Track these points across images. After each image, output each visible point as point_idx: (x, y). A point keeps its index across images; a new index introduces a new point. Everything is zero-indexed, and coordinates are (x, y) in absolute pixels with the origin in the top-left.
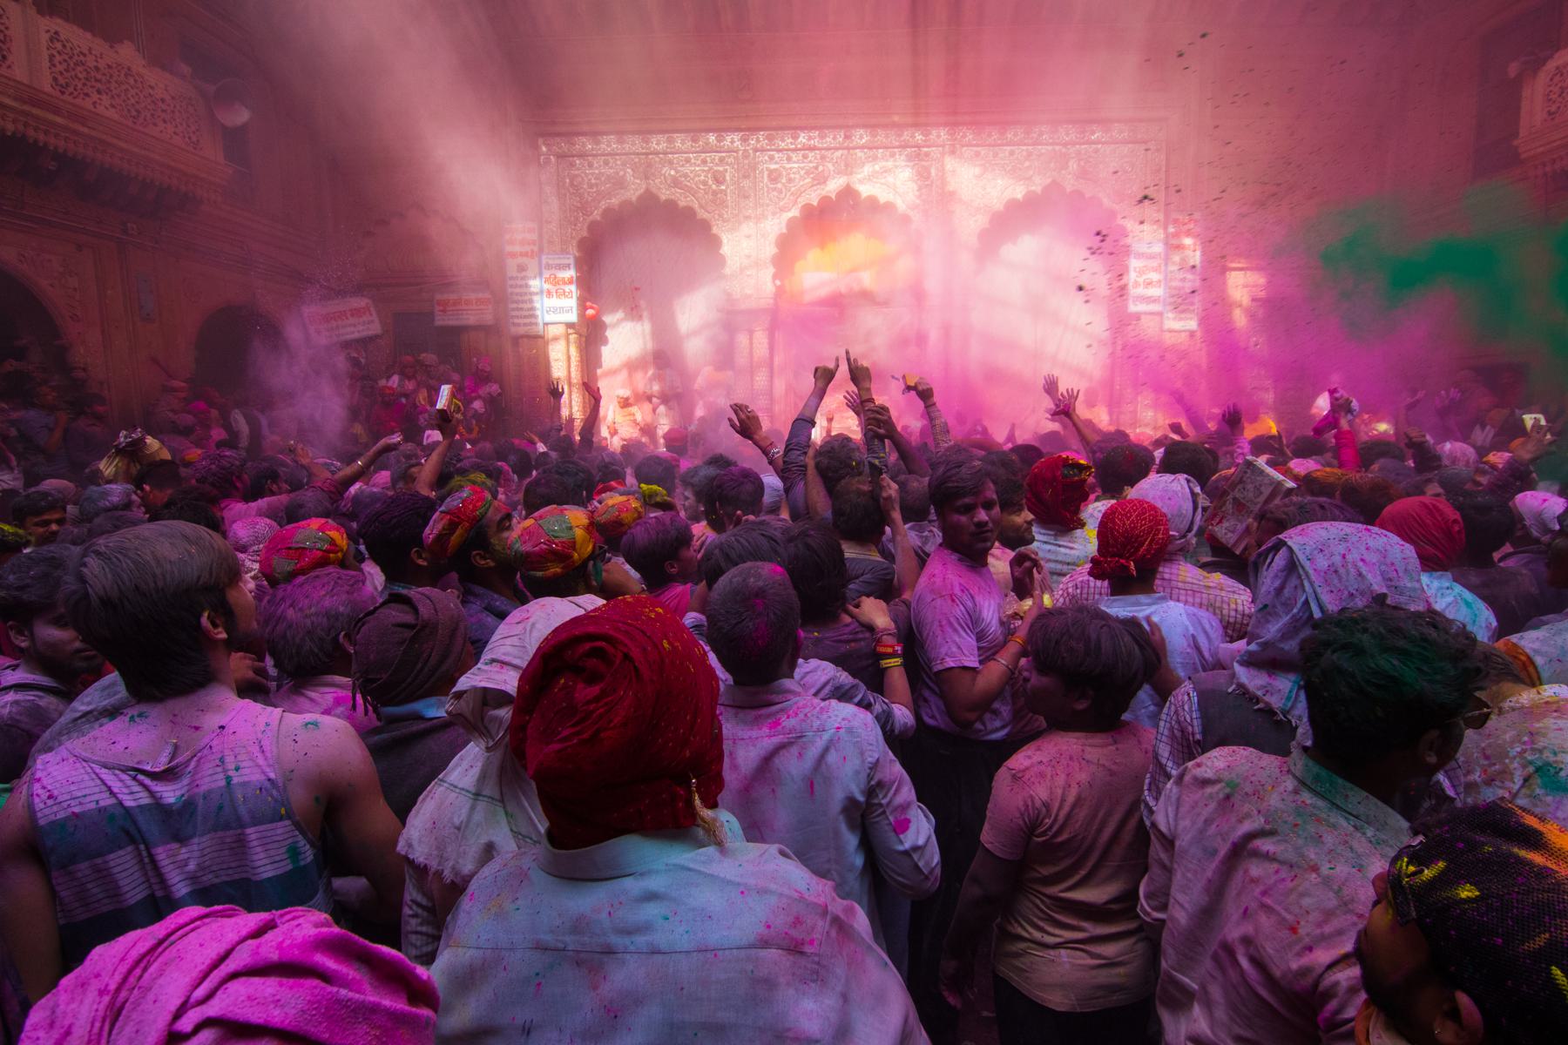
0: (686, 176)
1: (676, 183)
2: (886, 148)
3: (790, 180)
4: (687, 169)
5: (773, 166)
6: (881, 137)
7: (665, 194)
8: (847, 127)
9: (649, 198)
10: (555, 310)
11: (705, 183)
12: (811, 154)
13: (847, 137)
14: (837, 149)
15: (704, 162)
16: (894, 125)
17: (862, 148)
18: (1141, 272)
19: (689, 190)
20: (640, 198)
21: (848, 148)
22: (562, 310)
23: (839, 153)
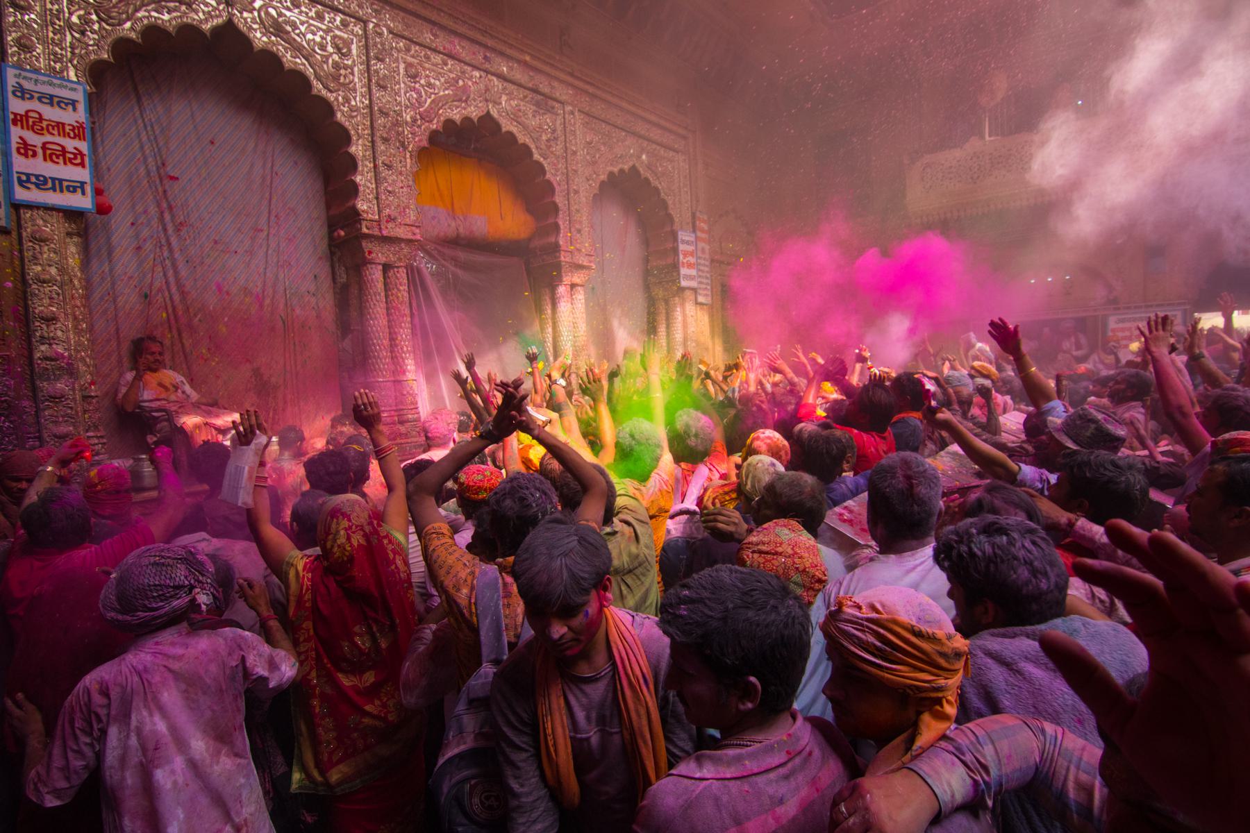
0: (295, 27)
1: (277, 28)
2: (520, 85)
3: (430, 85)
4: (291, 15)
5: (410, 59)
6: (518, 75)
7: (259, 38)
8: (486, 47)
9: (229, 33)
10: (42, 183)
11: (323, 48)
12: (450, 62)
13: (485, 58)
14: (475, 68)
15: (320, 17)
16: (525, 63)
17: (500, 76)
18: (685, 256)
19: (297, 49)
20: (216, 30)
21: (487, 72)
22: (58, 185)
23: (476, 74)
